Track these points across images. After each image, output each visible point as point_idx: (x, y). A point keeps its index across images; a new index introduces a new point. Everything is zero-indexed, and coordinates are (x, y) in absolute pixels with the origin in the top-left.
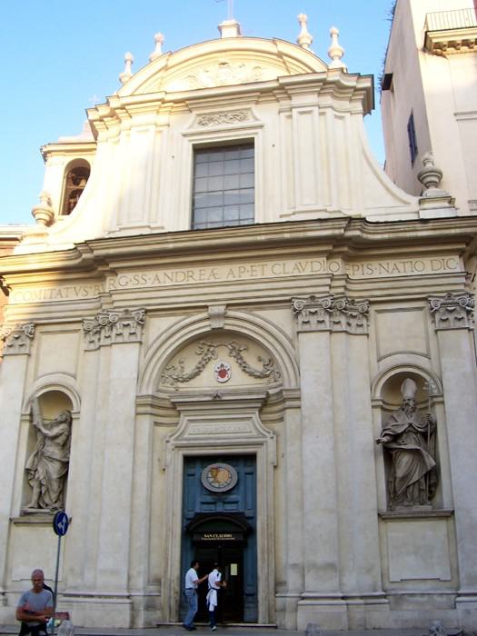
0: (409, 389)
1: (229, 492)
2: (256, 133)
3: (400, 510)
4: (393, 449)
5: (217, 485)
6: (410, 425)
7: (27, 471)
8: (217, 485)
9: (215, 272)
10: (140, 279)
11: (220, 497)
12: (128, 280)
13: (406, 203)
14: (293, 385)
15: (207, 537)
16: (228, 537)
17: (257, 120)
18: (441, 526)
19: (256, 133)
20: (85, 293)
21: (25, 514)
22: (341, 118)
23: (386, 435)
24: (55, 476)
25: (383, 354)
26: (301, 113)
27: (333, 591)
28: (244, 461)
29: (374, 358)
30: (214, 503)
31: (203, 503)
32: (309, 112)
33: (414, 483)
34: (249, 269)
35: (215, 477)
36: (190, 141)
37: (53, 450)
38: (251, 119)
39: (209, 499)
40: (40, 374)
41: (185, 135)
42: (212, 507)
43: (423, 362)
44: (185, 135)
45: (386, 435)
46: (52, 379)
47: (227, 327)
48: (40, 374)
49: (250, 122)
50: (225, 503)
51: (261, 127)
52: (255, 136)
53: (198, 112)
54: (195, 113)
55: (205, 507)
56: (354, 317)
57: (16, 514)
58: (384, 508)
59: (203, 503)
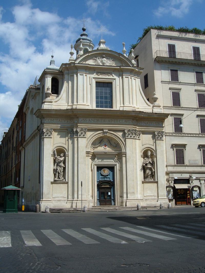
0: (149, 153)
1: (108, 175)
2: (113, 81)
3: (147, 180)
4: (145, 167)
5: (105, 174)
6: (150, 162)
7: (54, 170)
8: (105, 174)
9: (105, 120)
10: (85, 120)
11: (105, 176)
12: (82, 120)
13: (149, 106)
14: (124, 151)
15: (103, 186)
16: (108, 186)
17: (113, 76)
18: (156, 184)
19: (113, 81)
20: (67, 121)
21: (55, 181)
22: (135, 79)
23: (144, 164)
24: (62, 171)
25: (143, 144)
26: (126, 77)
27: (134, 198)
28: (112, 168)
29: (141, 145)
30: (104, 178)
31: (101, 178)
32: (128, 77)
33: (149, 175)
34: (114, 120)
35: (104, 172)
36: (95, 80)
37: (62, 164)
38: (112, 76)
39: (102, 177)
40: (55, 143)
41: (94, 78)
42: (104, 179)
44: (94, 78)
45: (144, 164)
46: (59, 145)
47: (108, 135)
48: (55, 143)
49: (111, 77)
50: (106, 178)
51: (115, 79)
52: (113, 82)
53: (97, 71)
54: (96, 72)
55: (102, 179)
56: (137, 135)
57: (53, 181)
58: (143, 180)
59: (101, 178)
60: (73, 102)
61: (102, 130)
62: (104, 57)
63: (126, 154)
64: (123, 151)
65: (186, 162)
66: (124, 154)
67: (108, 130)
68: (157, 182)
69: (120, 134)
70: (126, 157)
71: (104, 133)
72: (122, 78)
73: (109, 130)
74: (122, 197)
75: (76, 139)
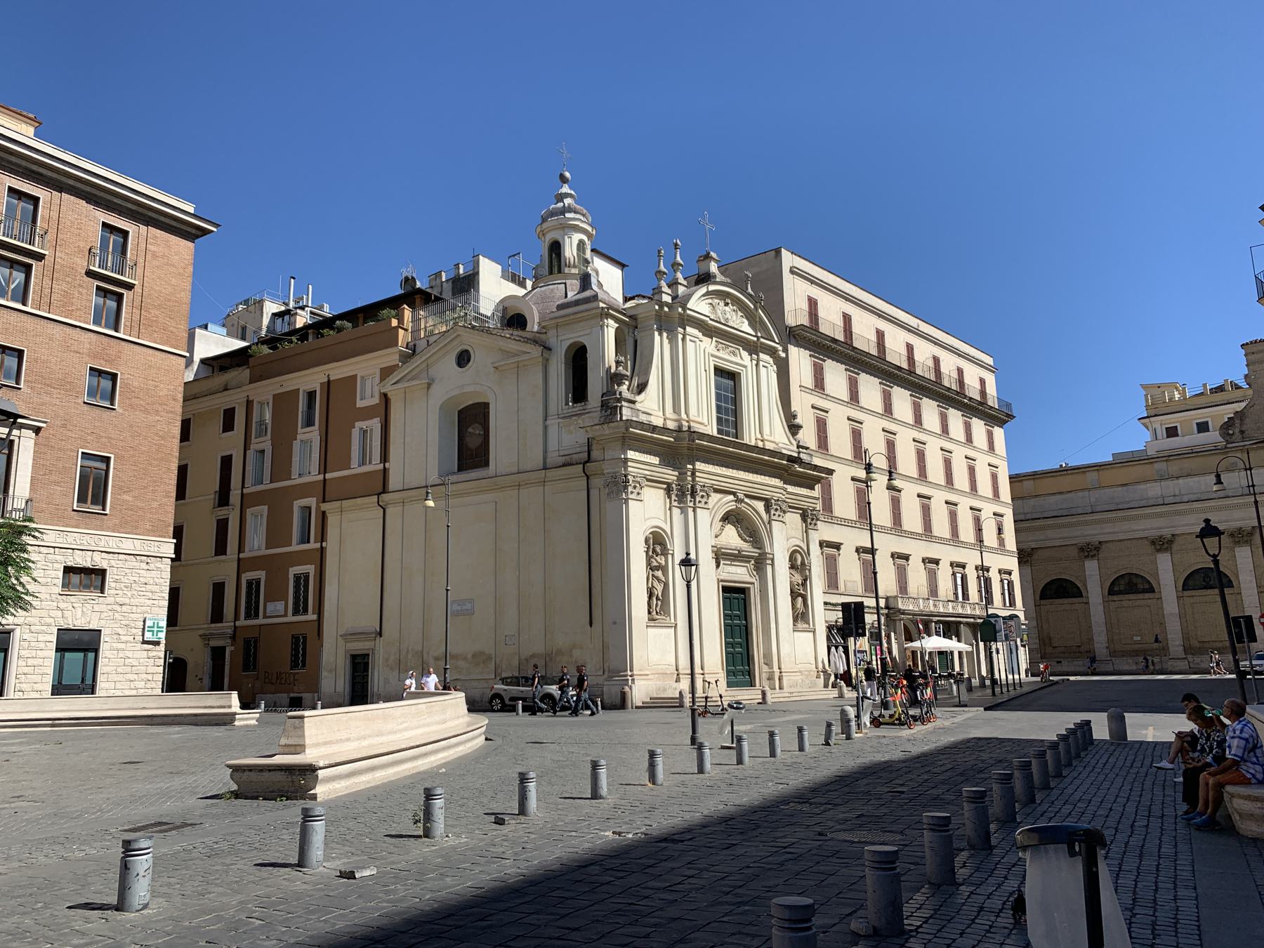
41: (712, 356)
43: (802, 544)
44: (712, 356)
49: (737, 360)
60: (676, 409)
61: (734, 494)
62: (727, 304)
63: (773, 560)
64: (768, 550)
65: (842, 588)
66: (769, 559)
67: (745, 495)
68: (814, 632)
69: (760, 506)
70: (773, 565)
71: (739, 501)
72: (757, 365)
73: (747, 496)
74: (769, 663)
75: (690, 510)
